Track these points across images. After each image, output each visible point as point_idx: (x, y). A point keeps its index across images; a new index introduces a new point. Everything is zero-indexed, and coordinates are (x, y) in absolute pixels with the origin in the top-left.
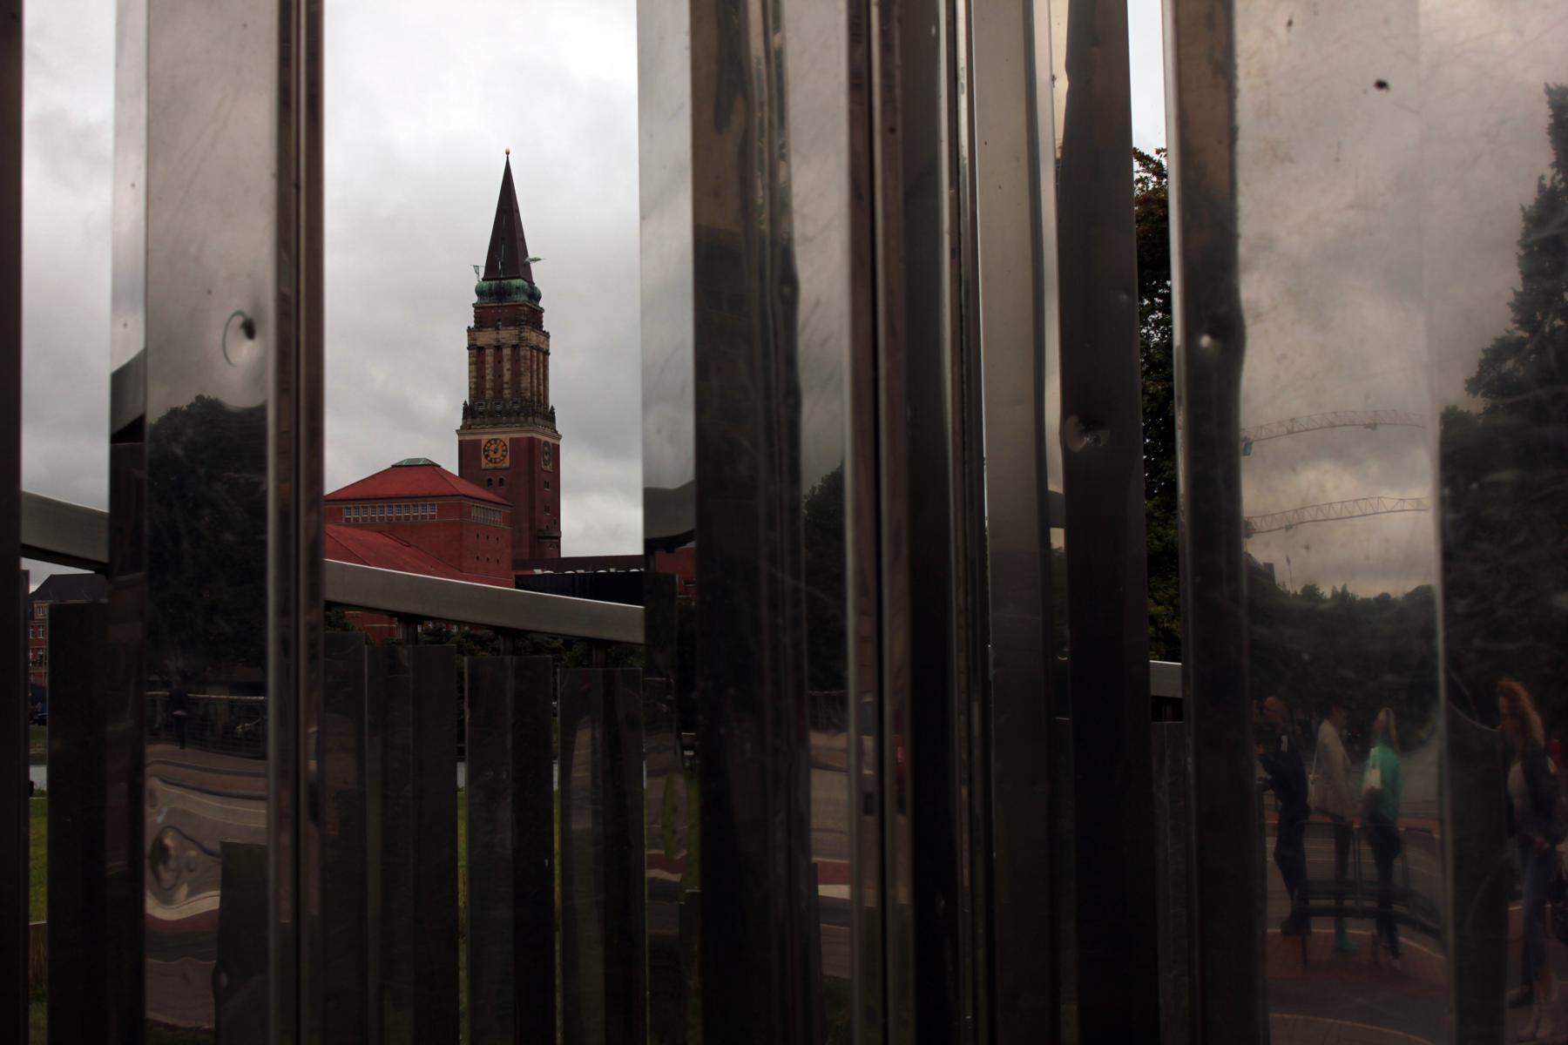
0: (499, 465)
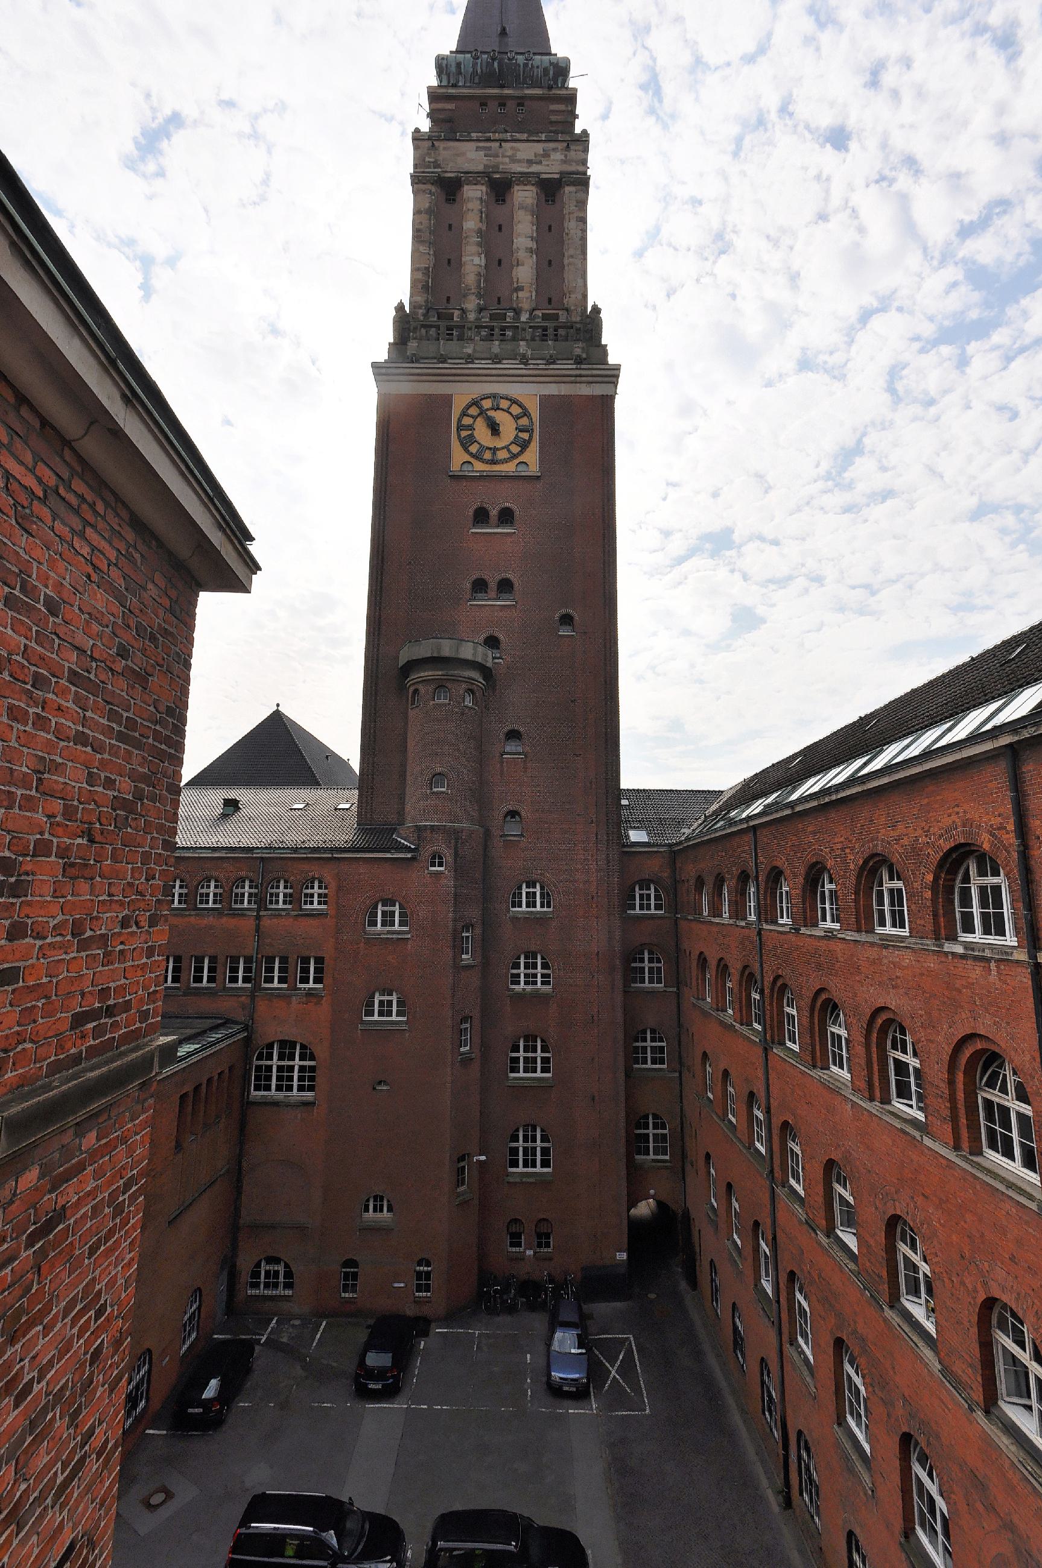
0: (510, 468)
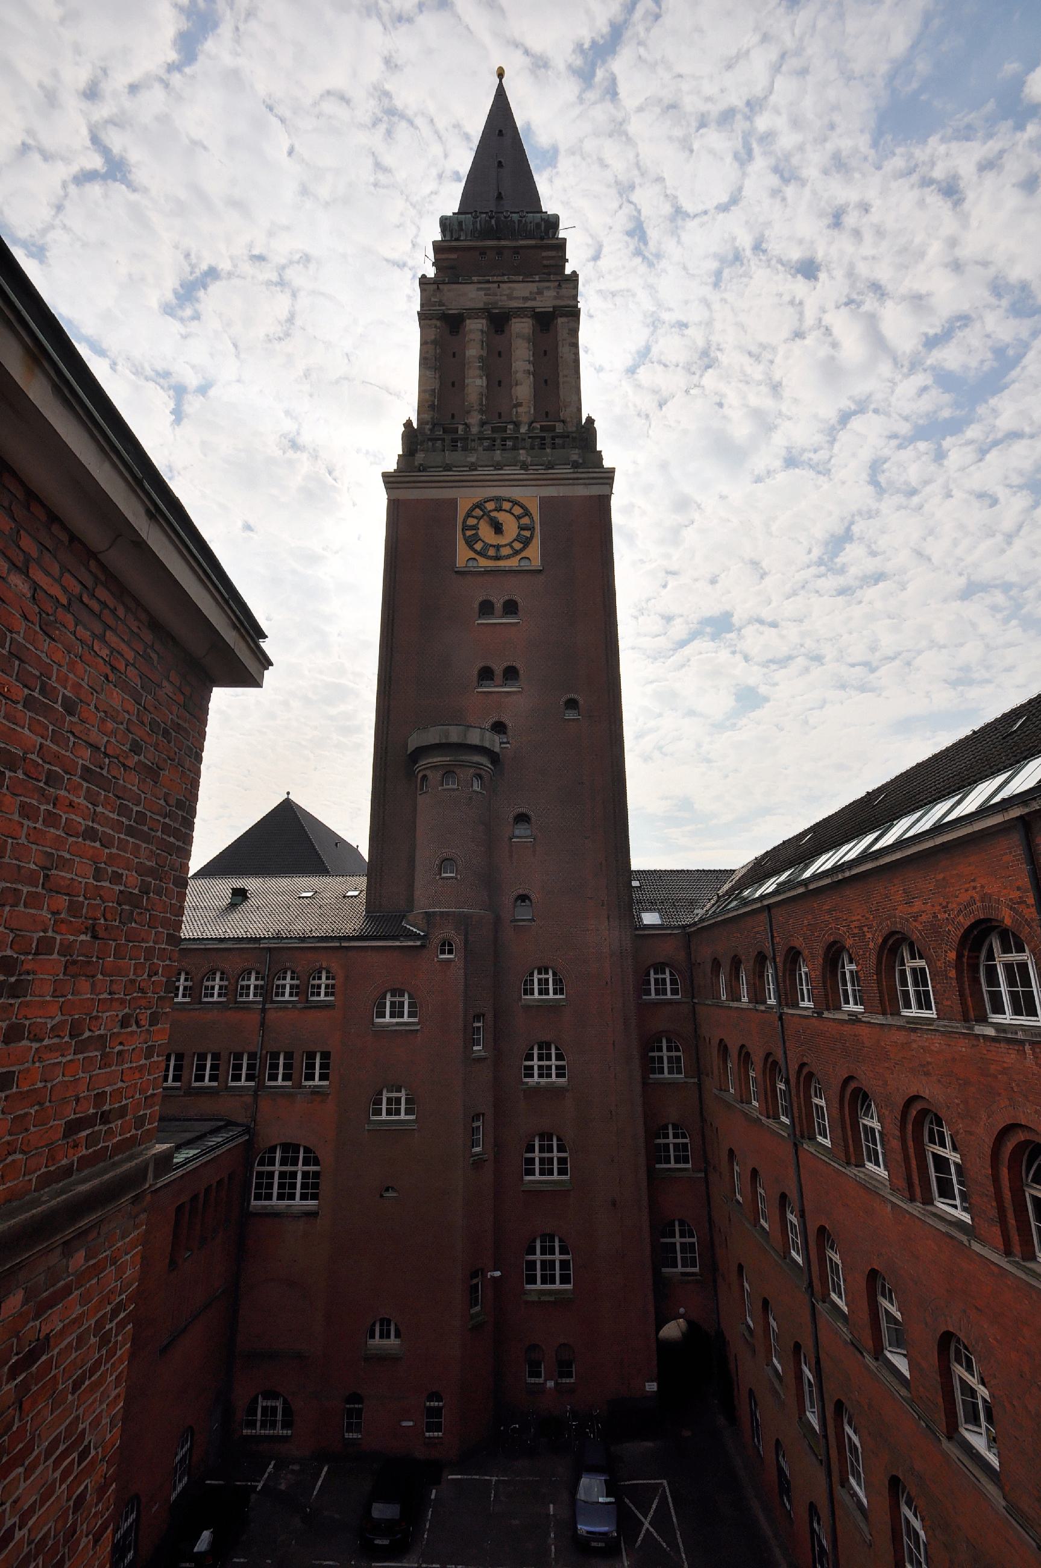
0: (513, 563)
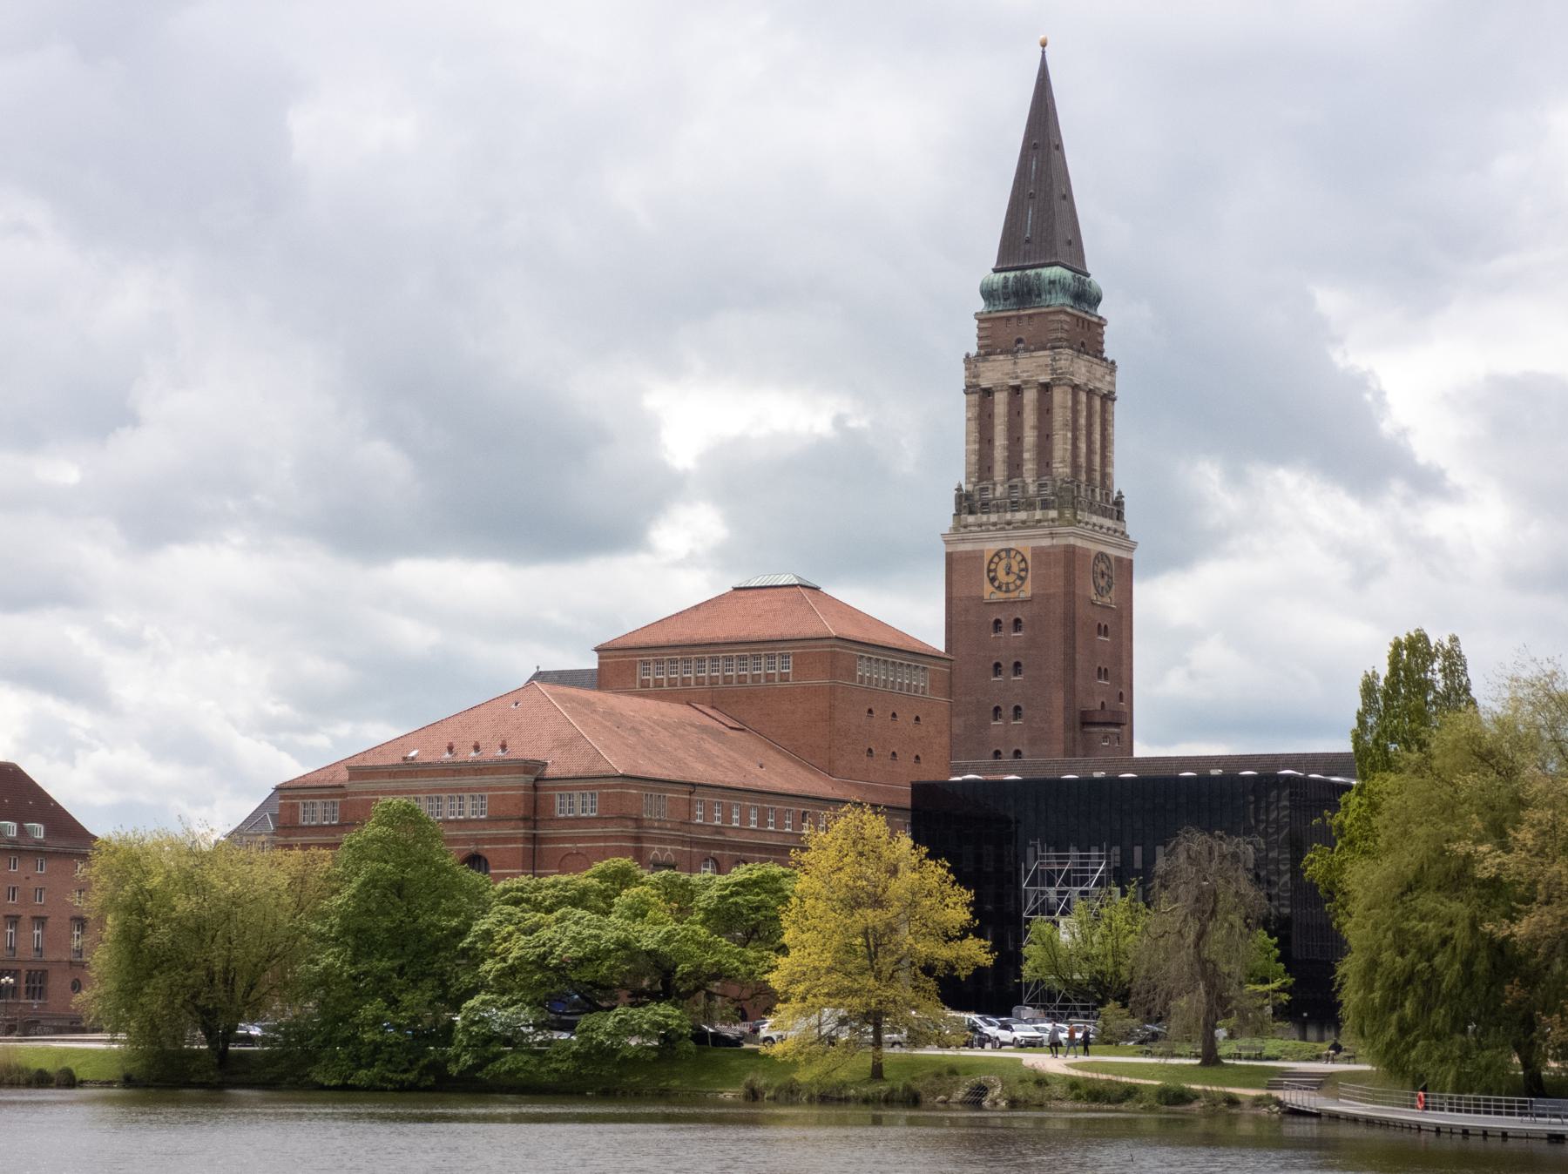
0: (1016, 594)
